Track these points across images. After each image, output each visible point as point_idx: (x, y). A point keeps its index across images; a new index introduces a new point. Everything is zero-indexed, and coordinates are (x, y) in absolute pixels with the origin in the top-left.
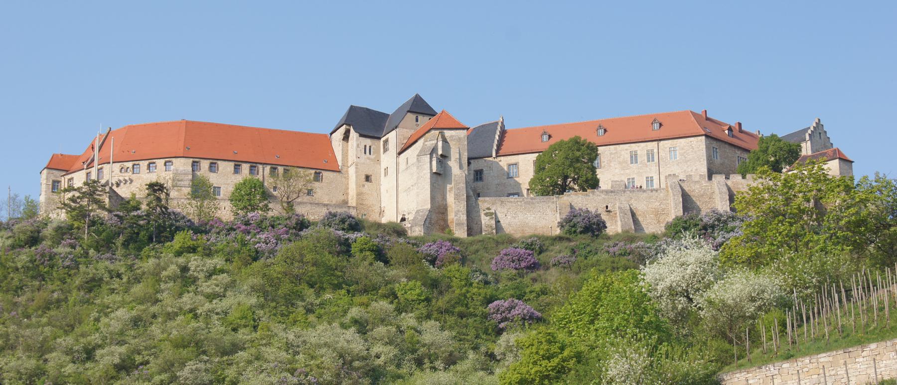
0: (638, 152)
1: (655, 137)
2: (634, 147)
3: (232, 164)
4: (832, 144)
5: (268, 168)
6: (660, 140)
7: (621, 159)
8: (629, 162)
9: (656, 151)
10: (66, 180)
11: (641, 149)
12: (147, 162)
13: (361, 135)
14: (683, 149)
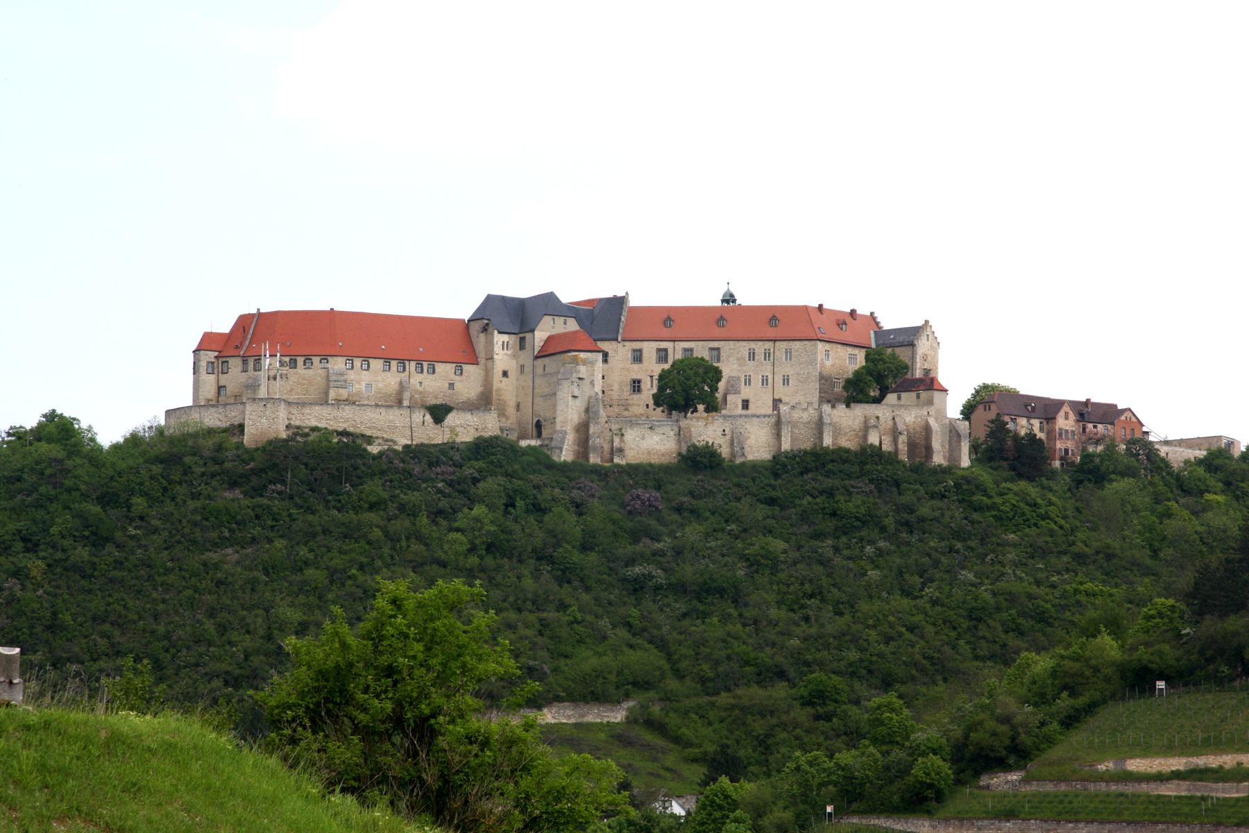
0: (756, 351)
1: (773, 336)
2: (752, 345)
3: (382, 361)
4: (939, 343)
5: (413, 364)
6: (775, 341)
7: (739, 356)
8: (747, 359)
9: (772, 350)
10: (220, 362)
11: (760, 348)
12: (303, 359)
13: (499, 332)
14: (797, 351)
